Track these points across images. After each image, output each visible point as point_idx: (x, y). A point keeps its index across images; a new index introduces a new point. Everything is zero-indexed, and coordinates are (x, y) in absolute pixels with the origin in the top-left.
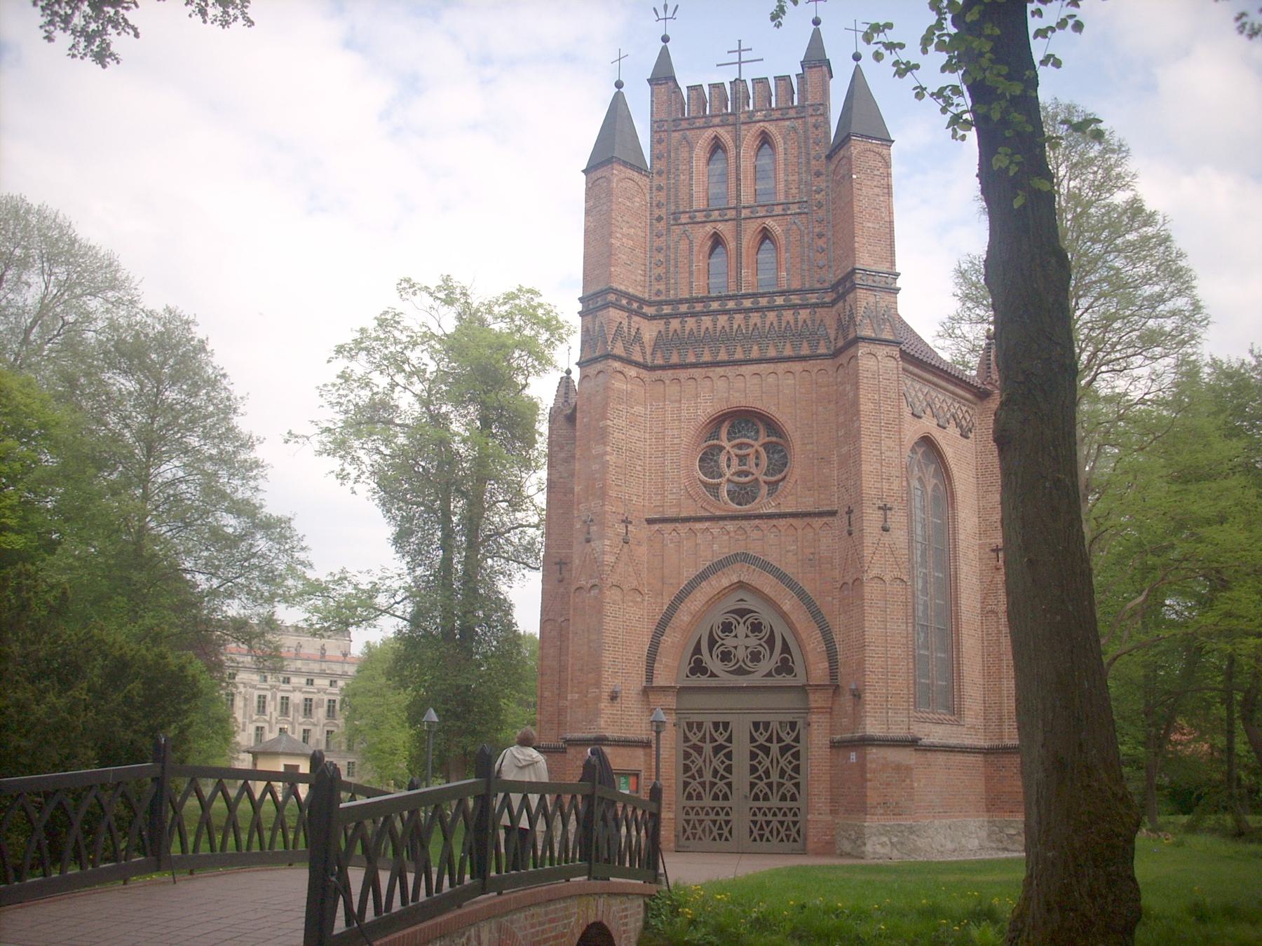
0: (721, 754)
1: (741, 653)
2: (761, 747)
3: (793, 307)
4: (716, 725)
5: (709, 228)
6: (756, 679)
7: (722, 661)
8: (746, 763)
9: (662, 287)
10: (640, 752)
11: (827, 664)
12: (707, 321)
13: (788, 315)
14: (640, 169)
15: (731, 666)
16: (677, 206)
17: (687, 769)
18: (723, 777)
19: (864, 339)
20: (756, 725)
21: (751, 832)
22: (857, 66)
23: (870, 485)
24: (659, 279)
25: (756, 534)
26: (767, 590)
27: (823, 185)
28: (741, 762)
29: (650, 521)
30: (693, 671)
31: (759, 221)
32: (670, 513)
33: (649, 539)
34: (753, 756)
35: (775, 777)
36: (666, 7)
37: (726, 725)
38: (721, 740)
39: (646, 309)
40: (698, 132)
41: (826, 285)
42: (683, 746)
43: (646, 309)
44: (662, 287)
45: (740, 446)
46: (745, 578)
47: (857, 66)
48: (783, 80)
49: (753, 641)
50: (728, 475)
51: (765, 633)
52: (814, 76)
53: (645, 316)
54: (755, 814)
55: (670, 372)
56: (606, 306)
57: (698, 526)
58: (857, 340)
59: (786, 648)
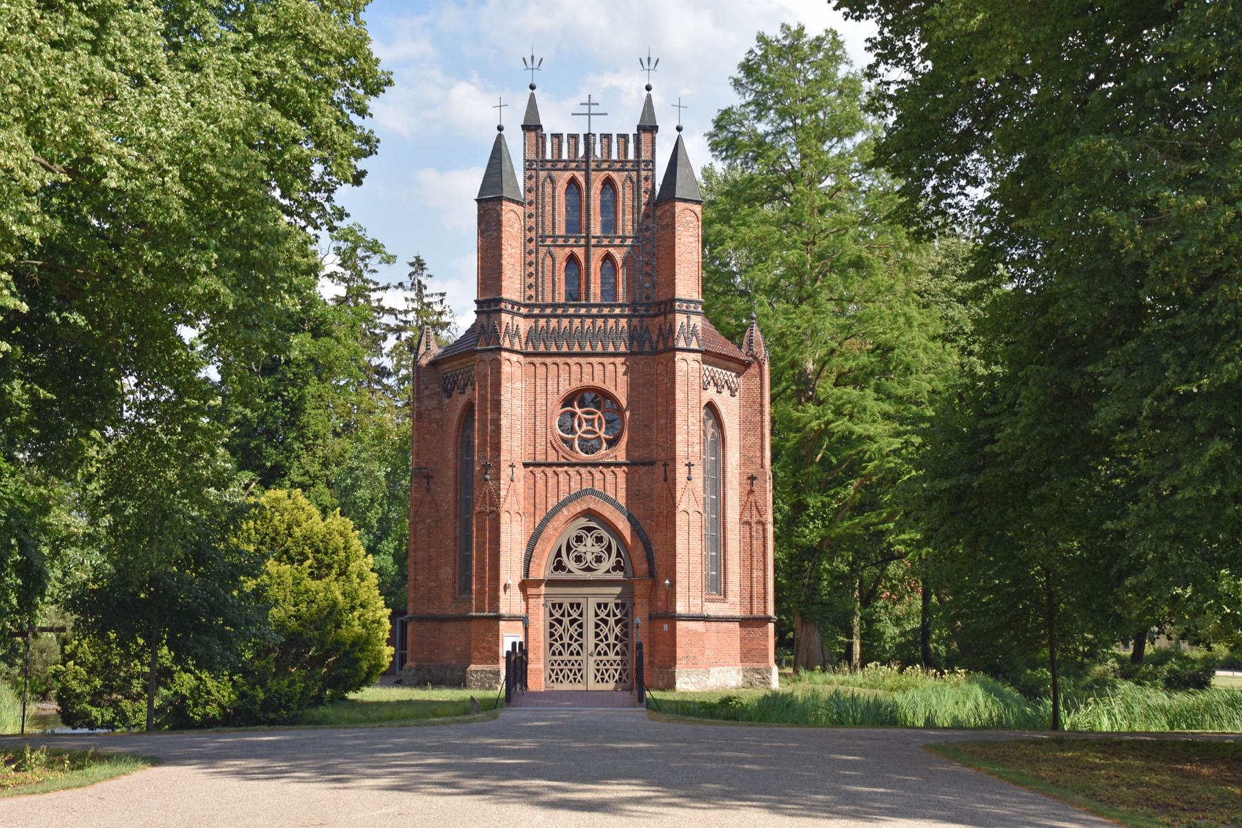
0: (575, 625)
1: (589, 557)
2: (602, 620)
4: (572, 605)
5: (567, 250)
6: (599, 574)
7: (576, 561)
9: (533, 293)
10: (520, 624)
11: (646, 566)
12: (565, 322)
16: (543, 230)
17: (552, 635)
18: (576, 640)
20: (599, 605)
21: (596, 677)
24: (530, 287)
26: (607, 515)
27: (651, 225)
28: (591, 630)
29: (526, 465)
30: (556, 569)
31: (604, 249)
32: (540, 458)
33: (525, 477)
34: (597, 626)
35: (566, 640)
37: (578, 605)
38: (575, 615)
40: (559, 173)
41: (651, 301)
42: (549, 620)
44: (533, 293)
45: (588, 413)
46: (592, 506)
48: (624, 137)
49: (597, 549)
50: (579, 433)
52: (645, 137)
54: (598, 665)
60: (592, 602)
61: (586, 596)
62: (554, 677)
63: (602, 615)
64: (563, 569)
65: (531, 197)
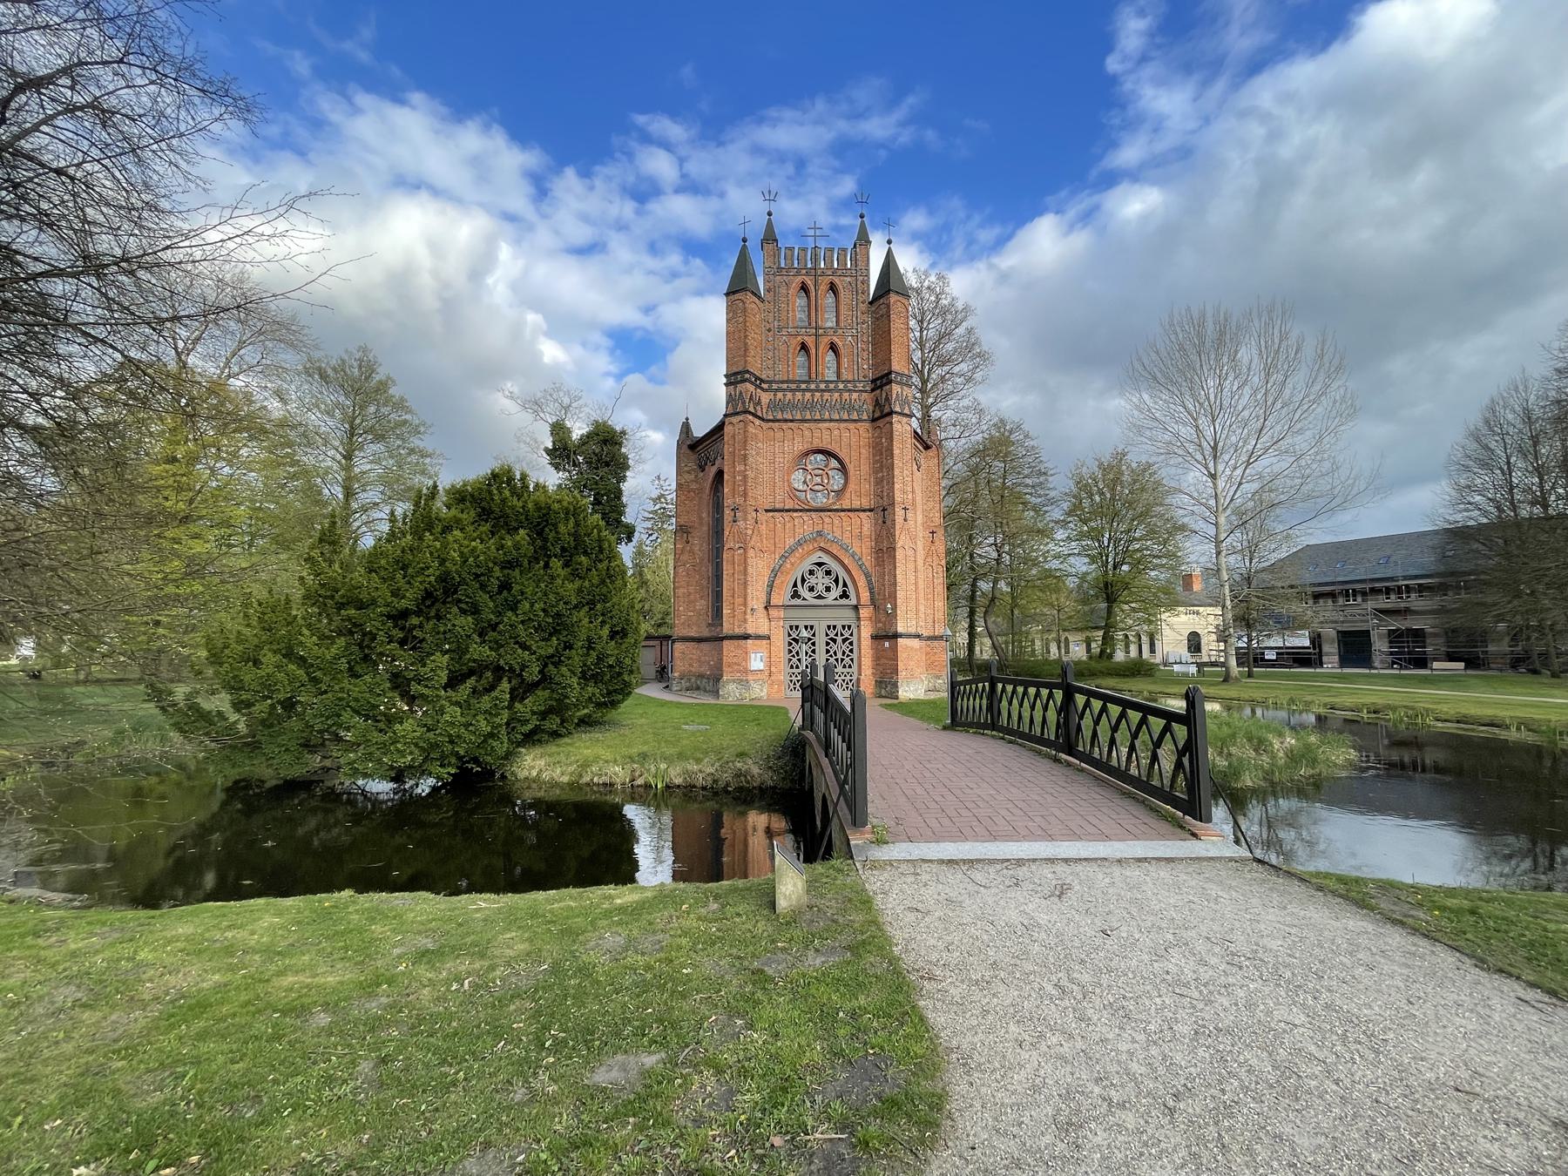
1: (820, 588)
3: (849, 390)
6: (829, 601)
8: (824, 648)
13: (846, 395)
14: (759, 297)
15: (814, 594)
17: (790, 651)
19: (896, 413)
20: (829, 627)
22: (890, 248)
23: (898, 497)
25: (827, 520)
29: (767, 511)
30: (793, 597)
34: (828, 644)
36: (770, 192)
37: (812, 627)
39: (763, 385)
42: (788, 639)
43: (763, 385)
47: (890, 248)
51: (833, 576)
53: (763, 389)
55: (777, 424)
56: (746, 380)
57: (795, 514)
58: (891, 413)
59: (845, 585)
60: (824, 625)
61: (820, 619)
62: (792, 686)
63: (832, 636)
64: (799, 597)
65: (769, 297)
